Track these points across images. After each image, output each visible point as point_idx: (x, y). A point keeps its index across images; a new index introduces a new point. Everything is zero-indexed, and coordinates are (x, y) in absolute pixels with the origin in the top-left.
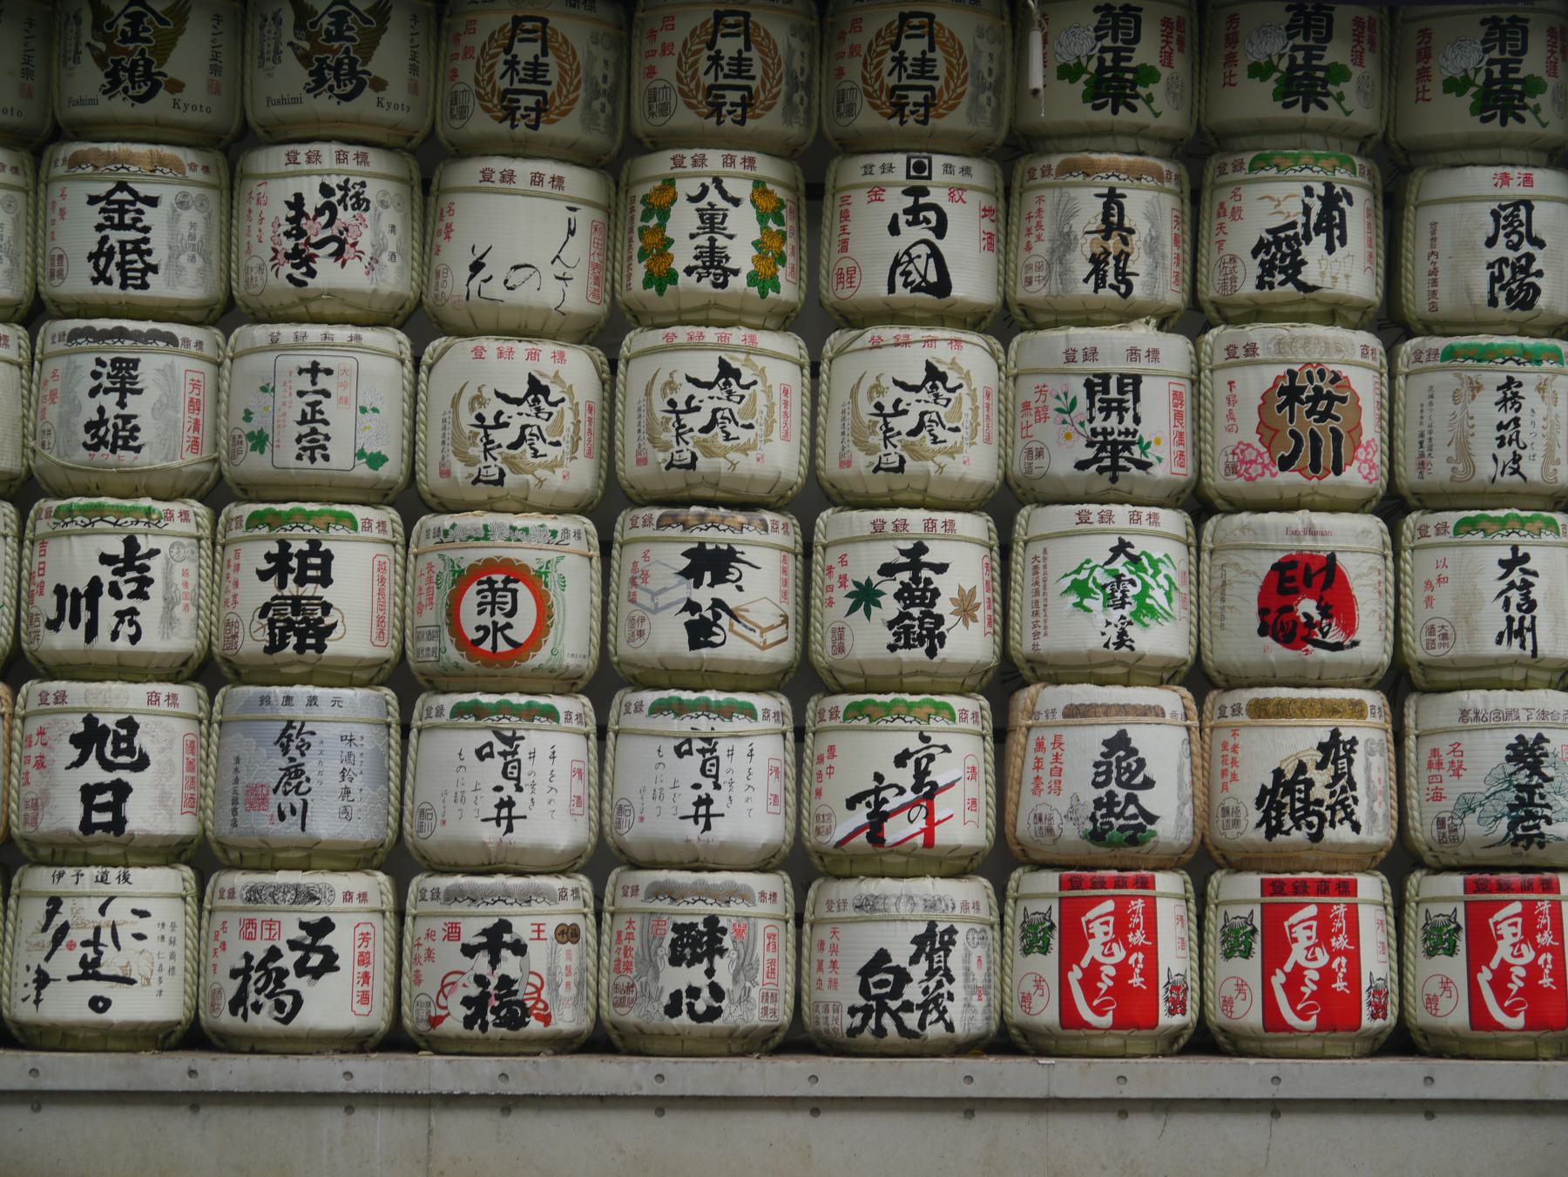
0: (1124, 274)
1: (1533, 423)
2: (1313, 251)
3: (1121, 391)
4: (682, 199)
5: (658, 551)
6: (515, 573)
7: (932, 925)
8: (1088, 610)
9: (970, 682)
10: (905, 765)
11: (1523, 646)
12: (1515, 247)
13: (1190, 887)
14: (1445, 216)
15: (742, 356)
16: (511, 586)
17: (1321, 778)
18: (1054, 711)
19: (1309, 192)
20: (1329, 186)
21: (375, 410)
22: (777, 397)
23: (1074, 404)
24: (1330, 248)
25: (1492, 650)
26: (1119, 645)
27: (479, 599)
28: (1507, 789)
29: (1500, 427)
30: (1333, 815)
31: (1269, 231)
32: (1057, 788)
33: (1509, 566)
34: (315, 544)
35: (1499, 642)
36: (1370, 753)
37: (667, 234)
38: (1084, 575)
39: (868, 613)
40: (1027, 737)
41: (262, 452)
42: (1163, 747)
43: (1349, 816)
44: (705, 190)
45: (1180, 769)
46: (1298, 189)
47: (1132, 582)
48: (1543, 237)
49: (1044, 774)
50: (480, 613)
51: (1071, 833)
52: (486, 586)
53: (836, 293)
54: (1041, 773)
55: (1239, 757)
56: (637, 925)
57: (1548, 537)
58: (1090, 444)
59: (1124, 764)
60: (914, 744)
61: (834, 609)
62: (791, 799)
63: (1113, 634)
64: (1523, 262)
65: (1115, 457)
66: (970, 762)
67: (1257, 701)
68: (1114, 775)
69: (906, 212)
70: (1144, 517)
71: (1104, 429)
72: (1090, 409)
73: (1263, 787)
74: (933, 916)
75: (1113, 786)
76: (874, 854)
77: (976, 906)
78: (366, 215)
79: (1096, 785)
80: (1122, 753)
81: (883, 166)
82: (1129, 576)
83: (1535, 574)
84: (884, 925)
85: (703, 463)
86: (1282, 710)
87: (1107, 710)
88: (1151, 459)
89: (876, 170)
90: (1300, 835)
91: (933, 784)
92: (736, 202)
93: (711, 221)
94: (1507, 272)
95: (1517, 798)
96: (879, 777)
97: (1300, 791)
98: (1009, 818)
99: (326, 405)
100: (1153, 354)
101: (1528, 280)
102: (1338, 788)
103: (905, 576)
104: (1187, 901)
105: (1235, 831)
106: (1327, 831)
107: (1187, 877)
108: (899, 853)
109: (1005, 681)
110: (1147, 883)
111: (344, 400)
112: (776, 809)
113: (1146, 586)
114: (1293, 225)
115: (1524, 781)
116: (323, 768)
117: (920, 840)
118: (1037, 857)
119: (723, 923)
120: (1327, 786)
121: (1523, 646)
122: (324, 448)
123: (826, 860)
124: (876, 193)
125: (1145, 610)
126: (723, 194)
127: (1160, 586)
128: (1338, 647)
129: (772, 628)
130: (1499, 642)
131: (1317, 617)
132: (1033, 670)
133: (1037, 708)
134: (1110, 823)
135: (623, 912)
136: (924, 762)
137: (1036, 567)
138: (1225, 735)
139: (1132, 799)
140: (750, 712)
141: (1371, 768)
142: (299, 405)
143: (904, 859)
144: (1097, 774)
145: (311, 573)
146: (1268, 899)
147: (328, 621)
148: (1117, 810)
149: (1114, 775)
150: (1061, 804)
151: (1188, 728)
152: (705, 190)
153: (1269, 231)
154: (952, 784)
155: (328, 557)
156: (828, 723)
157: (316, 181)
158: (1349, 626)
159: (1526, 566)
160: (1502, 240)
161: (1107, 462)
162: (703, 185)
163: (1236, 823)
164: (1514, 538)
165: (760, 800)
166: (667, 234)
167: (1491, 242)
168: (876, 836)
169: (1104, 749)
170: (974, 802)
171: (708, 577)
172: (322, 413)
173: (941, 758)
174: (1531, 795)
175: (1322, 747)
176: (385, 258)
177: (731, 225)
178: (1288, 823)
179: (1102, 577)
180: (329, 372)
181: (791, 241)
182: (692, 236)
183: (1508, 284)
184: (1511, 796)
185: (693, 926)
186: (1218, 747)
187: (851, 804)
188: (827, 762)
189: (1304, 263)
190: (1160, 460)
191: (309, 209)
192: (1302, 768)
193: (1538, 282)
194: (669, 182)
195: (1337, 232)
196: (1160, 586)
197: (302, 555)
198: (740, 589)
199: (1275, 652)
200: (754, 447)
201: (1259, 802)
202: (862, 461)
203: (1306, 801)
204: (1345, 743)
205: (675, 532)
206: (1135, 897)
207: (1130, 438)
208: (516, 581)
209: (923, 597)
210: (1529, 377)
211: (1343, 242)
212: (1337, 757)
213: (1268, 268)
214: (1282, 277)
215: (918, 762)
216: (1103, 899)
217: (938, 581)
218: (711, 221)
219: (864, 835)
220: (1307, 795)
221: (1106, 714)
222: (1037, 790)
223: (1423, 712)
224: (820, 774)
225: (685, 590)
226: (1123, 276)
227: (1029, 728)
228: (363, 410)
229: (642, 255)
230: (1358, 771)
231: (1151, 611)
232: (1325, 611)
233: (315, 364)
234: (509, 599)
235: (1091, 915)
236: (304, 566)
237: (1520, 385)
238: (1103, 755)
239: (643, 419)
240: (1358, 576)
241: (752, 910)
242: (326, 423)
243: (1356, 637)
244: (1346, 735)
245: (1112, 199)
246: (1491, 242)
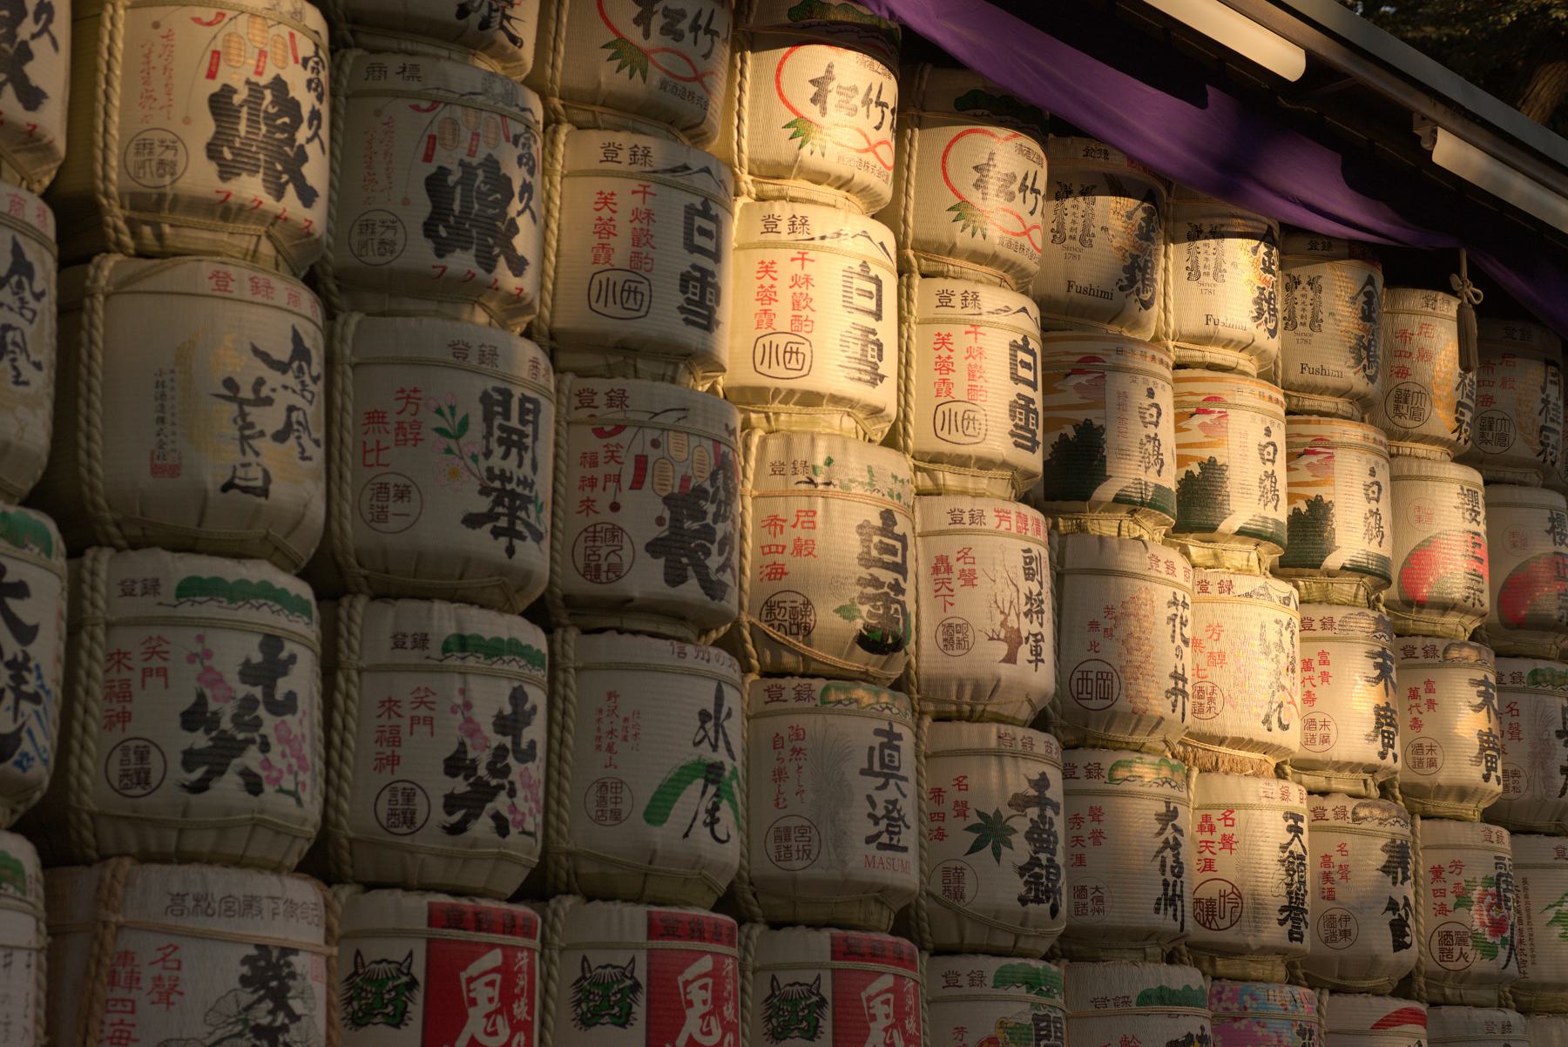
23: (464, 425)
58: (485, 491)
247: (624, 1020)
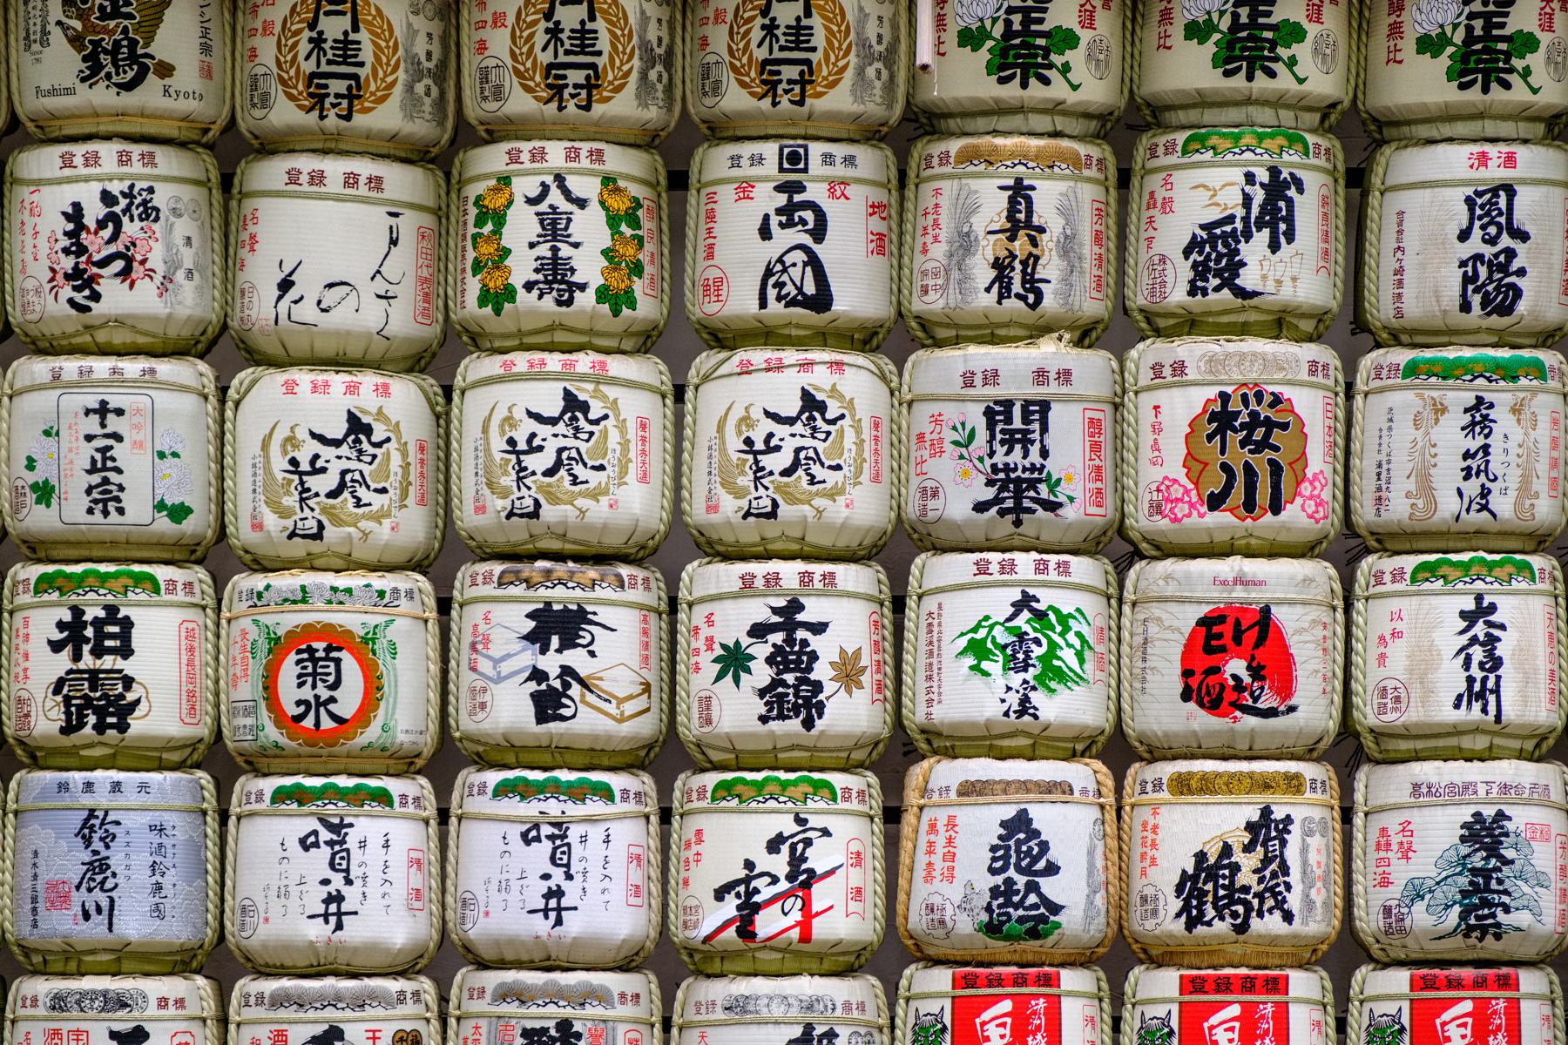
0: (1033, 281)
1: (1506, 451)
2: (1254, 250)
3: (1026, 420)
4: (519, 200)
5: (501, 613)
6: (338, 641)
7: (809, 1028)
8: (986, 674)
9: (858, 755)
10: (778, 852)
11: (1484, 711)
12: (1492, 241)
13: (1104, 985)
14: (1412, 202)
15: (590, 387)
16: (334, 654)
17: (1248, 863)
18: (948, 789)
19: (1250, 178)
20: (1274, 171)
21: (175, 455)
22: (632, 432)
24: (1274, 246)
25: (1447, 714)
26: (1021, 713)
27: (298, 670)
28: (1460, 874)
29: (1467, 455)
30: (1261, 903)
31: (1202, 227)
32: (950, 876)
33: (1470, 618)
34: (112, 610)
35: (1457, 706)
36: (1308, 833)
37: (503, 243)
38: (982, 633)
39: (737, 681)
40: (919, 818)
41: (48, 506)
42: (1069, 830)
43: (1280, 904)
44: (545, 189)
45: (1091, 853)
46: (1237, 175)
47: (1038, 642)
48: (1527, 228)
49: (937, 860)
50: (300, 685)
51: (965, 925)
52: (305, 656)
53: (704, 308)
54: (933, 858)
55: (1159, 838)
56: (484, 1031)
57: (1520, 584)
58: (990, 483)
59: (1024, 848)
60: (788, 826)
61: (701, 676)
62: (655, 889)
63: (1014, 700)
64: (1502, 258)
65: (1018, 497)
66: (854, 847)
67: (1180, 775)
68: (1013, 860)
69: (779, 211)
70: (1052, 566)
71: (1006, 465)
72: (990, 442)
73: (1184, 872)
74: (809, 1017)
75: (1012, 873)
76: (743, 950)
77: (862, 1007)
78: (155, 227)
79: (993, 871)
80: (1022, 836)
81: (752, 158)
82: (1032, 635)
83: (1502, 627)
84: (754, 1028)
85: (549, 512)
86: (1206, 785)
87: (1007, 786)
88: (1061, 499)
89: (745, 162)
90: (1222, 927)
91: (811, 872)
92: (582, 203)
93: (553, 228)
94: (1483, 271)
95: (1471, 883)
96: (749, 865)
97: (1224, 877)
98: (900, 908)
99: (119, 451)
100: (1065, 376)
101: (1507, 280)
102: (1267, 873)
103: (778, 638)
104: (1101, 1000)
105: (1154, 921)
106: (1255, 922)
107: (1101, 974)
108: (772, 949)
109: (897, 753)
110: (1051, 981)
111: (138, 445)
112: (638, 901)
113: (1053, 646)
114: (1230, 219)
115: (1480, 865)
116: (130, 864)
117: (795, 934)
118: (931, 951)
119: (578, 1027)
120: (1255, 872)
121: (1484, 711)
122: (118, 500)
123: (697, 957)
124: (745, 189)
125: (1053, 674)
126: (567, 193)
127: (1069, 645)
128: (1271, 713)
129: (631, 697)
130: (1457, 706)
131: (1247, 679)
132: (929, 742)
133: (930, 786)
134: (1008, 914)
135: (469, 1016)
136: (800, 847)
137: (930, 625)
138: (1144, 814)
139: (1032, 887)
140: (606, 793)
141: (1308, 851)
142: (87, 451)
143: (780, 956)
144: (994, 859)
145: (108, 643)
146: (1187, 998)
147: (130, 697)
148: (1016, 899)
149: (1013, 860)
150: (955, 893)
151: (1102, 807)
152: (545, 189)
153: (1202, 227)
154: (831, 872)
155: (127, 624)
156: (696, 804)
157: (96, 188)
158: (1285, 688)
159: (1491, 618)
160: (1477, 232)
161: (1009, 504)
162: (543, 184)
163: (1155, 913)
164: (1479, 585)
165: (618, 891)
166: (503, 243)
167: (1464, 236)
168: (746, 930)
169: (1002, 831)
170: (859, 891)
171: (555, 641)
172: (113, 460)
173: (820, 843)
174: (1488, 879)
175: (1250, 827)
176: (180, 276)
177: (576, 231)
178: (1210, 912)
179: (1002, 636)
180: (119, 412)
181: (649, 247)
182: (532, 246)
183: (1484, 285)
184: (1463, 881)
185: (545, 1030)
186: (1138, 827)
187: (720, 894)
188: (695, 848)
189: (1243, 264)
190: (1072, 499)
191: (90, 221)
192: (1227, 850)
193: (1520, 282)
194: (505, 180)
195: (1283, 227)
196: (1069, 645)
197: (97, 622)
198: (592, 654)
199: (1199, 720)
200: (606, 492)
201: (1179, 889)
202: (730, 506)
203: (1230, 887)
204: (1277, 822)
205: (518, 590)
206: (1037, 996)
207: (1036, 475)
208: (339, 649)
209: (799, 662)
210: (1502, 397)
211: (1290, 238)
212: (1268, 839)
213: (1201, 271)
214: (1217, 281)
215: (793, 848)
216: (999, 998)
217: (816, 643)
218: (553, 228)
219: (733, 928)
220: (1232, 882)
221: (1005, 792)
222: (929, 878)
223: (1382, 786)
224: (687, 861)
225: (529, 656)
226: (1033, 285)
227: (921, 808)
228: (162, 455)
229: (477, 267)
230: (1292, 854)
231: (1060, 676)
232: (1256, 672)
233: (104, 403)
234: (332, 669)
235: (986, 1016)
236: (100, 635)
237: (1491, 406)
238: (1000, 837)
239: (480, 461)
240: (1299, 631)
241: (610, 1013)
242: (119, 471)
243: (1292, 702)
244: (1279, 813)
245: (1019, 193)
246: (1464, 236)
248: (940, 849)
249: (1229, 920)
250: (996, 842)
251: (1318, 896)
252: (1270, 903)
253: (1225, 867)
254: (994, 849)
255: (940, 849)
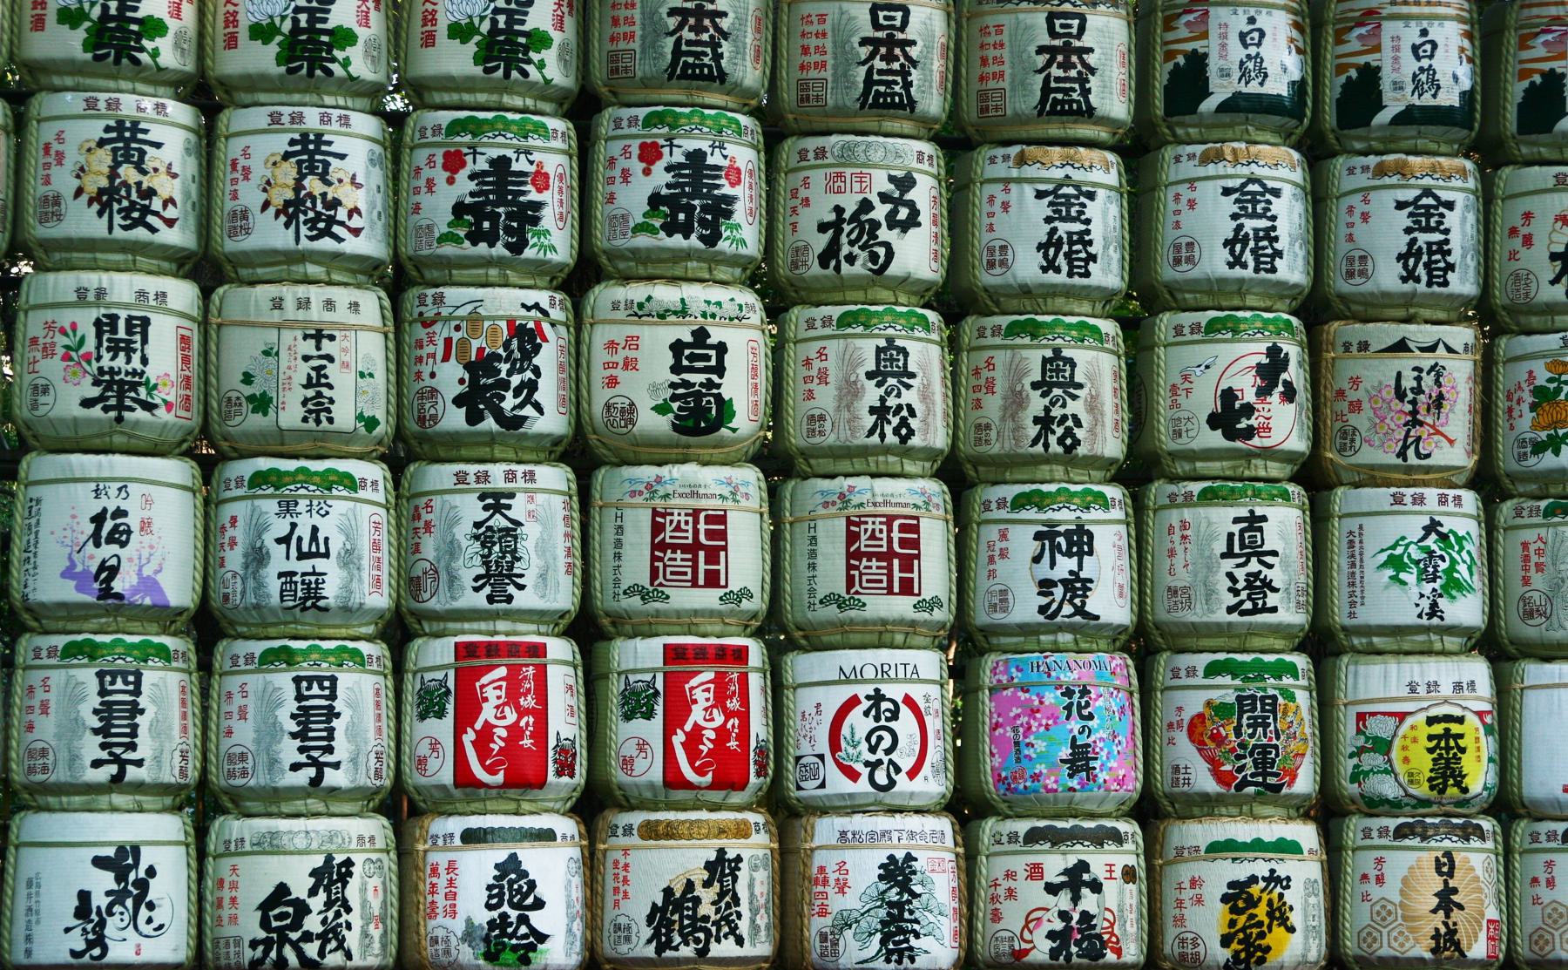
17: (707, 896)
18: (452, 835)
30: (719, 930)
36: (755, 868)
73: (654, 905)
75: (506, 908)
79: (489, 907)
90: (687, 951)
97: (688, 909)
102: (723, 905)
106: (713, 945)
120: (713, 903)
139: (523, 920)
144: (490, 897)
148: (510, 930)
150: (458, 926)
163: (628, 939)
169: (497, 873)
175: (709, 866)
178: (677, 939)
192: (690, 885)
201: (650, 919)
203: (694, 918)
204: (730, 861)
212: (723, 875)
238: (495, 878)
244: (731, 855)
247: (649, 715)
248: (442, 890)
249: (693, 945)
250: (492, 882)
251: (762, 920)
252: (726, 929)
253: (689, 900)
254: (490, 888)
255: (442, 890)
